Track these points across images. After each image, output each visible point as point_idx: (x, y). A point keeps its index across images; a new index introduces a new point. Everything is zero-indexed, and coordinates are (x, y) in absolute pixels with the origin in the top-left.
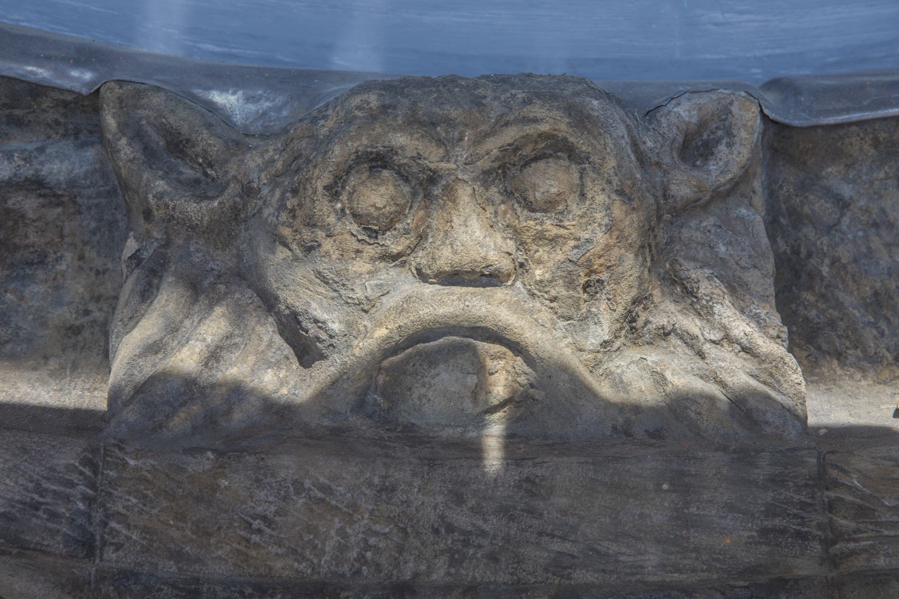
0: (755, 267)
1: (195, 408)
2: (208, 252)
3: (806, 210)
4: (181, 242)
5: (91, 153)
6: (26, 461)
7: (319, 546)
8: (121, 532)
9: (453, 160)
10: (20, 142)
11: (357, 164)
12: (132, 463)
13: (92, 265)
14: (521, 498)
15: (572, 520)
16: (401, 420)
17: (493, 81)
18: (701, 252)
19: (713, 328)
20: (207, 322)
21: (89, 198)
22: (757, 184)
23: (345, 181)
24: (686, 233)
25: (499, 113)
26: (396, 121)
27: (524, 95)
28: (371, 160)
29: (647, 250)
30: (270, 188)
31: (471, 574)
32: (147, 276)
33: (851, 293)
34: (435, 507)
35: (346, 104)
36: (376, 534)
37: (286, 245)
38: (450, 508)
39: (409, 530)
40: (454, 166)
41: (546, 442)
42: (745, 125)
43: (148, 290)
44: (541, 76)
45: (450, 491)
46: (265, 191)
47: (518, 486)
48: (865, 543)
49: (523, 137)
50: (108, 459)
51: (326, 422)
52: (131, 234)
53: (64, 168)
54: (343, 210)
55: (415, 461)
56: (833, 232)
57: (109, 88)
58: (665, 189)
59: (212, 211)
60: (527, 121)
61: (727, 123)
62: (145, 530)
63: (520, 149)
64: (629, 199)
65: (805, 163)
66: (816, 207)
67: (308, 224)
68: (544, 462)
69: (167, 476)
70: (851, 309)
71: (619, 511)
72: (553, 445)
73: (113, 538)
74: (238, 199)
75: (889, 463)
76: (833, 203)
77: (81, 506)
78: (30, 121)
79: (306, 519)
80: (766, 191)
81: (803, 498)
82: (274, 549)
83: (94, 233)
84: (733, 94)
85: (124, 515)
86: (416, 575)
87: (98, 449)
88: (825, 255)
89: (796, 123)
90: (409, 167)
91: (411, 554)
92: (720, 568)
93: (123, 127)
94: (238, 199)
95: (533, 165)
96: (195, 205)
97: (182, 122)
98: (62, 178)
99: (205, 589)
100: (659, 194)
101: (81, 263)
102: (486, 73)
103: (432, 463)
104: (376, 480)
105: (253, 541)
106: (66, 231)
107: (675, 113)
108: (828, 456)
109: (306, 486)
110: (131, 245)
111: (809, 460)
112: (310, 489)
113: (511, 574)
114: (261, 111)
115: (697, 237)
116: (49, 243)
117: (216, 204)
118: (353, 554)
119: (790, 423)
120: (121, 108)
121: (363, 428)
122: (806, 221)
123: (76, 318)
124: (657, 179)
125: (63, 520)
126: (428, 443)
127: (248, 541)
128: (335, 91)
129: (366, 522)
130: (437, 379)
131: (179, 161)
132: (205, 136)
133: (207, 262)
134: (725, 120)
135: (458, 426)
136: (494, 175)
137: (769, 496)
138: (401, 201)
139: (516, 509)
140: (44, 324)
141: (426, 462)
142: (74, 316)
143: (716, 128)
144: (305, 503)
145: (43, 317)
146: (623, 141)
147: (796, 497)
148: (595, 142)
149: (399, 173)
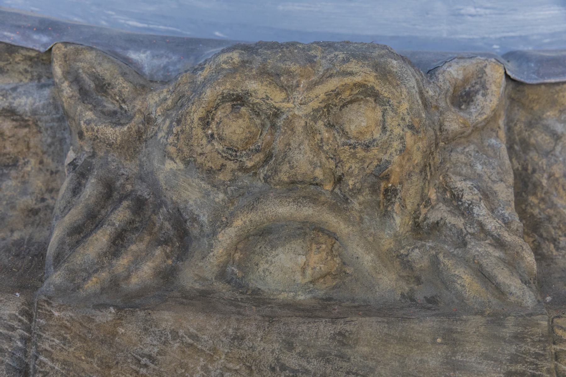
0: (502, 181)
1: (104, 274)
2: (121, 162)
3: (532, 141)
4: (102, 154)
5: (47, 92)
8: (47, 364)
9: (292, 101)
11: (223, 102)
12: (56, 314)
13: (48, 168)
14: (335, 347)
15: (371, 364)
16: (250, 285)
17: (321, 46)
18: (464, 169)
23: (214, 114)
25: (326, 68)
26: (251, 72)
28: (233, 100)
30: (163, 118)
32: (78, 178)
33: (562, 197)
35: (217, 60)
36: (229, 370)
37: (172, 159)
39: (253, 368)
40: (293, 106)
41: (353, 304)
42: (495, 82)
43: (78, 188)
44: (356, 43)
45: (284, 341)
46: (160, 120)
47: (333, 338)
50: (39, 311)
51: (197, 286)
52: (71, 147)
53: (28, 102)
54: (212, 135)
55: (259, 318)
58: (441, 125)
61: (483, 80)
62: (65, 363)
64: (417, 132)
65: (532, 109)
66: (539, 138)
67: (188, 145)
68: (352, 321)
69: (81, 324)
70: (562, 209)
71: (405, 358)
72: (358, 307)
73: (42, 368)
74: (141, 126)
76: (551, 136)
77: (20, 344)
78: (8, 70)
79: (179, 358)
80: (506, 127)
81: (537, 351)
83: (49, 146)
84: (487, 60)
85: (50, 352)
87: (33, 303)
88: (544, 171)
90: (260, 105)
93: (66, 74)
94: (141, 126)
95: (349, 106)
96: (111, 129)
97: (106, 72)
98: (27, 109)
100: (437, 128)
101: (41, 166)
103: (271, 319)
104: (231, 331)
105: (141, 373)
106: (32, 144)
108: (555, 320)
109: (180, 334)
110: (71, 155)
111: (542, 322)
112: (182, 337)
114: (162, 65)
115: (462, 159)
116: (19, 152)
117: (126, 128)
119: (527, 293)
120: (66, 61)
121: (224, 291)
122: (532, 148)
123: (36, 204)
124: (436, 118)
125: (6, 354)
126: (269, 303)
129: (223, 361)
130: (276, 258)
131: (104, 98)
132: (121, 81)
133: (119, 169)
134: (481, 78)
135: (290, 292)
136: (321, 112)
137: (513, 349)
138: (254, 129)
139: (330, 354)
140: (13, 207)
141: (267, 319)
142: (34, 202)
143: (476, 83)
144: (179, 347)
145: (13, 203)
146: (414, 91)
147: (532, 349)
148: (394, 90)
149: (253, 110)
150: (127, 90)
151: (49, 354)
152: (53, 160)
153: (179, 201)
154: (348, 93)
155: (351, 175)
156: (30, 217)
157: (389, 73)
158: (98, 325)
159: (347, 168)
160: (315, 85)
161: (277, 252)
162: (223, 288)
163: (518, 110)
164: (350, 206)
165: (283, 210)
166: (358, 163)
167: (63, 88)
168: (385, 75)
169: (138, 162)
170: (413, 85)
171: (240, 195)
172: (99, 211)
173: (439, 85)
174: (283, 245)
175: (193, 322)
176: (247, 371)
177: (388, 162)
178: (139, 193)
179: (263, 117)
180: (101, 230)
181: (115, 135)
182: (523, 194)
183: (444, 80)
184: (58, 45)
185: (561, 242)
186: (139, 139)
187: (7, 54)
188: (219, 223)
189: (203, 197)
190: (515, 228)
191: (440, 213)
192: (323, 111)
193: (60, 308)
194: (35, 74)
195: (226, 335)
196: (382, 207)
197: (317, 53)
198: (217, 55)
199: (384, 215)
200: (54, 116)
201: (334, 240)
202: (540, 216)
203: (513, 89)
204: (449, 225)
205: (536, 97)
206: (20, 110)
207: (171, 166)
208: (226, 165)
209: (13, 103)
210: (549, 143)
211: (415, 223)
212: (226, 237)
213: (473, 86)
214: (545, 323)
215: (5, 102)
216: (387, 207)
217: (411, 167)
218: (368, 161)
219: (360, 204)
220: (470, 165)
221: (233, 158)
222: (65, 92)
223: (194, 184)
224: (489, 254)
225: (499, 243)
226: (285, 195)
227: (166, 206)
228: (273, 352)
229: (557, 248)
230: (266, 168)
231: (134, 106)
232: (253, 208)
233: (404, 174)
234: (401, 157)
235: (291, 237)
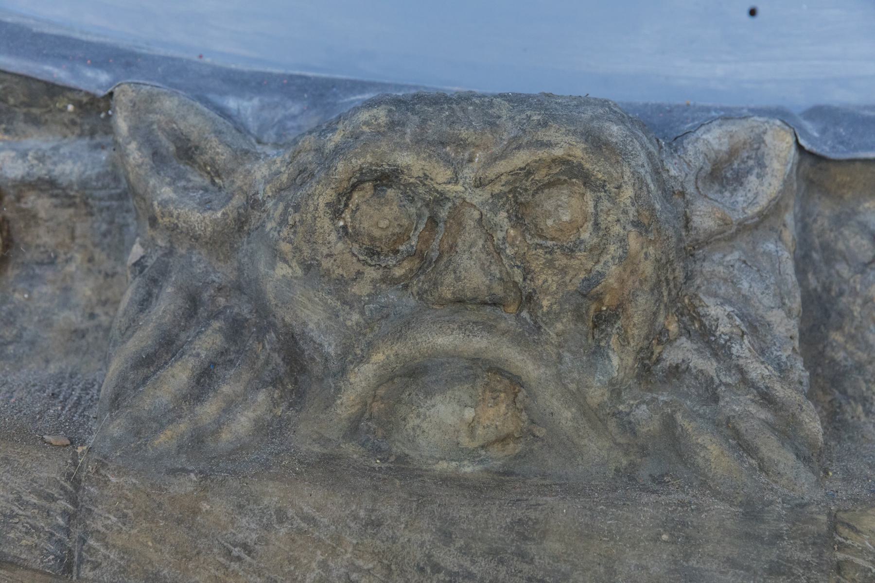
2: (210, 263)
3: (841, 246)
4: (184, 252)
5: (104, 156)
7: (299, 578)
10: (37, 141)
12: (114, 480)
14: (513, 540)
15: (564, 567)
16: (394, 449)
20: (203, 336)
21: (101, 199)
22: (789, 218)
24: (707, 267)
27: (539, 117)
29: (665, 284)
32: (147, 285)
35: (355, 119)
36: (358, 569)
37: (286, 261)
39: (393, 567)
41: (543, 482)
42: (779, 156)
43: (147, 300)
44: (562, 97)
46: (270, 204)
49: (536, 162)
51: (316, 449)
52: (138, 239)
53: (76, 169)
57: (123, 91)
58: (688, 220)
59: (215, 222)
61: (759, 152)
63: (533, 174)
64: (647, 231)
65: (841, 197)
66: (852, 242)
67: (309, 241)
68: (539, 505)
71: (614, 562)
73: (91, 556)
77: (61, 521)
80: (799, 225)
83: (104, 235)
84: (768, 122)
89: (833, 156)
93: (134, 130)
94: (242, 211)
95: (546, 191)
97: (192, 129)
101: (90, 265)
104: (362, 513)
106: (78, 232)
107: (704, 140)
109: (290, 515)
110: (137, 251)
115: (720, 272)
119: (803, 475)
121: (355, 456)
123: (82, 322)
126: (420, 476)
128: (352, 102)
129: (349, 555)
130: (432, 410)
131: (188, 167)
133: (207, 273)
134: (758, 148)
135: (452, 460)
138: (405, 222)
142: (80, 319)
143: (748, 157)
149: (404, 193)
150: (223, 157)
151: (102, 538)
152: (108, 256)
153: (294, 323)
154: (544, 172)
155: (546, 292)
159: (541, 282)
160: (496, 159)
161: (433, 401)
163: (819, 198)
164: (544, 337)
165: (443, 339)
167: (128, 151)
168: (600, 148)
169: (236, 264)
170: (640, 163)
171: (382, 317)
172: (177, 335)
173: (687, 160)
176: (384, 572)
177: (601, 275)
178: (236, 310)
179: (419, 205)
180: (180, 363)
181: (203, 224)
182: (822, 327)
183: (696, 153)
184: (123, 86)
186: (239, 231)
188: (350, 357)
189: (330, 318)
190: (796, 379)
191: (683, 352)
192: (507, 197)
194: (87, 127)
195: (355, 519)
196: (590, 341)
197: (504, 110)
198: (356, 109)
199: (594, 353)
200: (113, 191)
202: (846, 363)
204: (694, 371)
205: (848, 179)
206: (63, 181)
207: (284, 272)
208: (363, 273)
209: (54, 170)
211: (644, 365)
212: (362, 378)
213: (744, 162)
214: (823, 518)
216: (600, 341)
217: (637, 283)
219: (557, 335)
220: (732, 282)
221: (373, 263)
222: (131, 157)
223: (317, 299)
225: (766, 398)
226: (447, 318)
227: (275, 332)
229: (868, 413)
231: (233, 182)
232: (400, 336)
233: (626, 292)
234: (621, 269)
235: (453, 381)
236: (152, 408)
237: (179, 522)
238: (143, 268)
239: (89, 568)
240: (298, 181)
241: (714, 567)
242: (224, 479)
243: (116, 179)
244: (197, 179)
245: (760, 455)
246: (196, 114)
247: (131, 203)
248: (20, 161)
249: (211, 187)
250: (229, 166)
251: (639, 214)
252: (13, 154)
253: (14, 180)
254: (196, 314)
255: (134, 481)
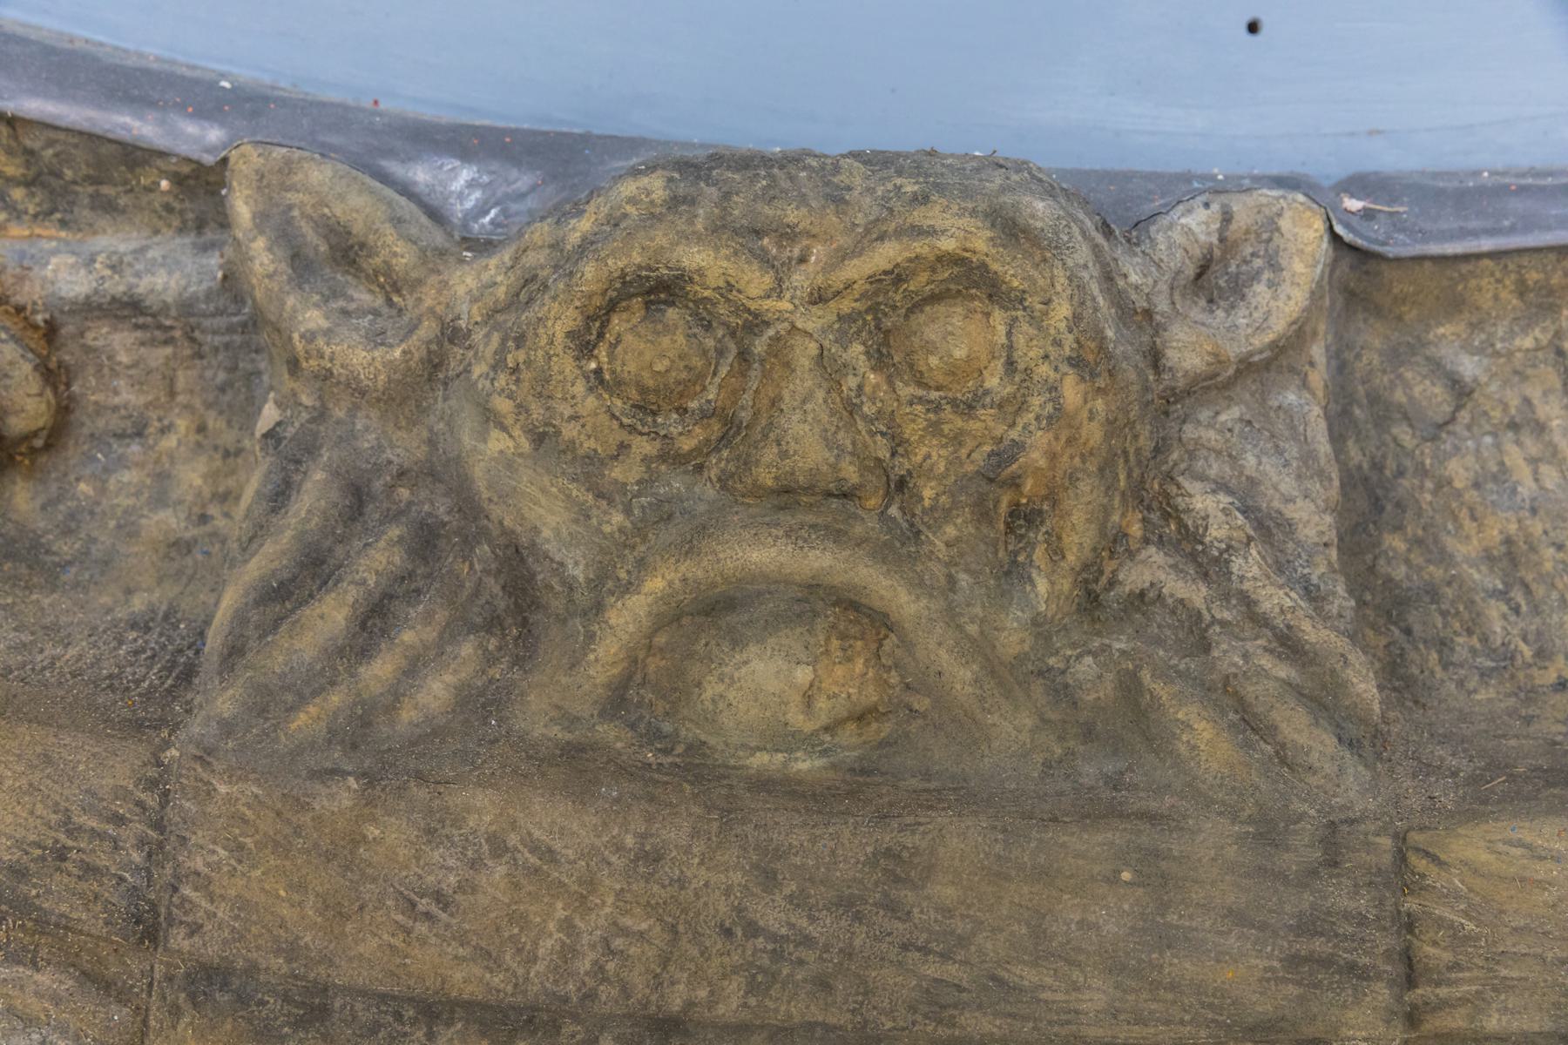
3: (1399, 396)
5: (214, 261)
6: (48, 777)
7: (528, 947)
9: (788, 296)
10: (113, 240)
12: (223, 789)
13: (219, 442)
14: (876, 884)
15: (961, 927)
16: (683, 733)
17: (865, 163)
18: (1215, 466)
19: (1226, 597)
21: (215, 333)
22: (1317, 351)
24: (1189, 431)
26: (693, 223)
27: (916, 188)
30: (485, 330)
31: (783, 1008)
34: (728, 892)
35: (613, 194)
36: (625, 932)
37: (504, 428)
38: (753, 895)
39: (681, 928)
42: (1302, 251)
44: (952, 155)
45: (756, 866)
46: (478, 336)
47: (872, 862)
48: (1466, 988)
49: (910, 260)
51: (556, 731)
52: (272, 395)
53: (173, 284)
56: (1444, 435)
57: (243, 155)
59: (388, 364)
60: (918, 232)
61: (1272, 246)
62: (242, 905)
63: (906, 281)
65: (1400, 318)
66: (1417, 390)
67: (540, 395)
68: (920, 824)
69: (279, 814)
71: (1044, 916)
73: (186, 913)
75: (1518, 852)
77: (137, 857)
80: (1334, 363)
82: (453, 949)
83: (222, 389)
84: (1284, 198)
85: (208, 877)
86: (690, 1004)
89: (1390, 251)
90: (714, 305)
91: (682, 969)
92: (1213, 1021)
93: (261, 219)
94: (434, 347)
95: (928, 309)
99: (337, 1004)
101: (200, 438)
102: (856, 148)
104: (629, 841)
107: (1183, 226)
109: (510, 844)
110: (269, 415)
111: (1378, 840)
113: (853, 1011)
118: (585, 965)
119: (1351, 771)
121: (619, 745)
127: (408, 932)
129: (608, 910)
130: (743, 670)
131: (349, 278)
133: (380, 448)
134: (1270, 240)
135: (777, 750)
142: (183, 525)
143: (1253, 255)
148: (1036, 274)
149: (695, 314)
152: (229, 422)
153: (519, 529)
154: (923, 277)
156: (173, 559)
157: (1023, 232)
158: (318, 819)
159: (919, 458)
162: (618, 738)
164: (926, 548)
165: (760, 553)
166: (944, 446)
167: (252, 253)
169: (425, 434)
170: (1082, 262)
171: (662, 519)
172: (330, 550)
174: (761, 641)
175: (548, 818)
177: (1018, 446)
178: (426, 508)
179: (720, 333)
180: (333, 595)
183: (1169, 248)
185: (1458, 648)
187: (123, 168)
188: (610, 584)
189: (576, 521)
190: (1335, 611)
191: (1151, 569)
192: (865, 322)
193: (231, 776)
194: (190, 216)
195: (618, 850)
196: (1001, 554)
197: (856, 177)
198: (619, 178)
199: (1008, 574)
200: (235, 319)
201: (883, 631)
203: (1351, 267)
204: (1170, 601)
207: (501, 446)
208: (629, 446)
210: (1440, 404)
211: (1089, 593)
212: (628, 616)
213: (1245, 262)
214: (1386, 842)
215: (118, 284)
216: (1016, 553)
217: (1077, 460)
218: (970, 444)
219: (948, 545)
220: (1230, 456)
221: (646, 430)
223: (554, 490)
224: (1262, 673)
225: (1289, 645)
226: (767, 519)
228: (728, 892)
230: (725, 453)
231: (419, 299)
232: (691, 548)
233: (1059, 474)
234: (1050, 435)
236: (287, 670)
237: (329, 857)
238: (279, 441)
239: (182, 935)
240: (523, 297)
241: (1208, 924)
242: (403, 788)
243: (239, 299)
244: (363, 296)
245: (1279, 738)
246: (360, 192)
247: (264, 337)
248: (83, 272)
249: (385, 310)
250: (414, 275)
251: (1081, 346)
252: (71, 260)
253: (74, 303)
254: (361, 514)
255: (255, 790)
